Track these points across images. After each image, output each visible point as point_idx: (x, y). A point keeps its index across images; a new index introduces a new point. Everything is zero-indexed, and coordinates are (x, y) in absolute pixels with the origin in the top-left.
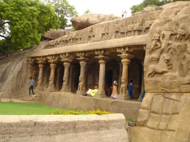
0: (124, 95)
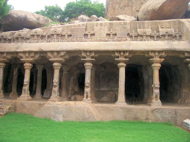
0: (159, 101)
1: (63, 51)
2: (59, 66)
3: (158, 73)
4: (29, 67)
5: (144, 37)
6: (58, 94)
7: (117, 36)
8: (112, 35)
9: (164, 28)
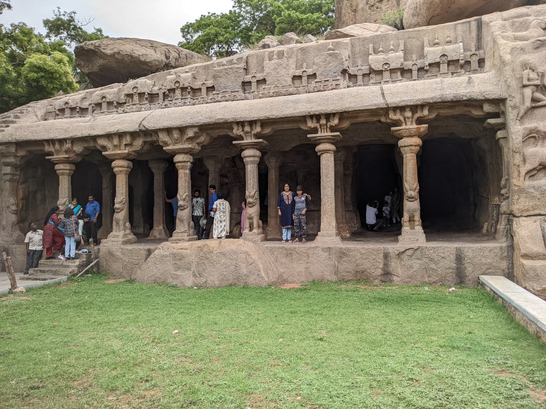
0: (419, 229)
1: (192, 126)
2: (187, 162)
3: (415, 162)
4: (123, 169)
5: (387, 75)
6: (189, 225)
7: (316, 80)
8: (306, 78)
9: (438, 44)
